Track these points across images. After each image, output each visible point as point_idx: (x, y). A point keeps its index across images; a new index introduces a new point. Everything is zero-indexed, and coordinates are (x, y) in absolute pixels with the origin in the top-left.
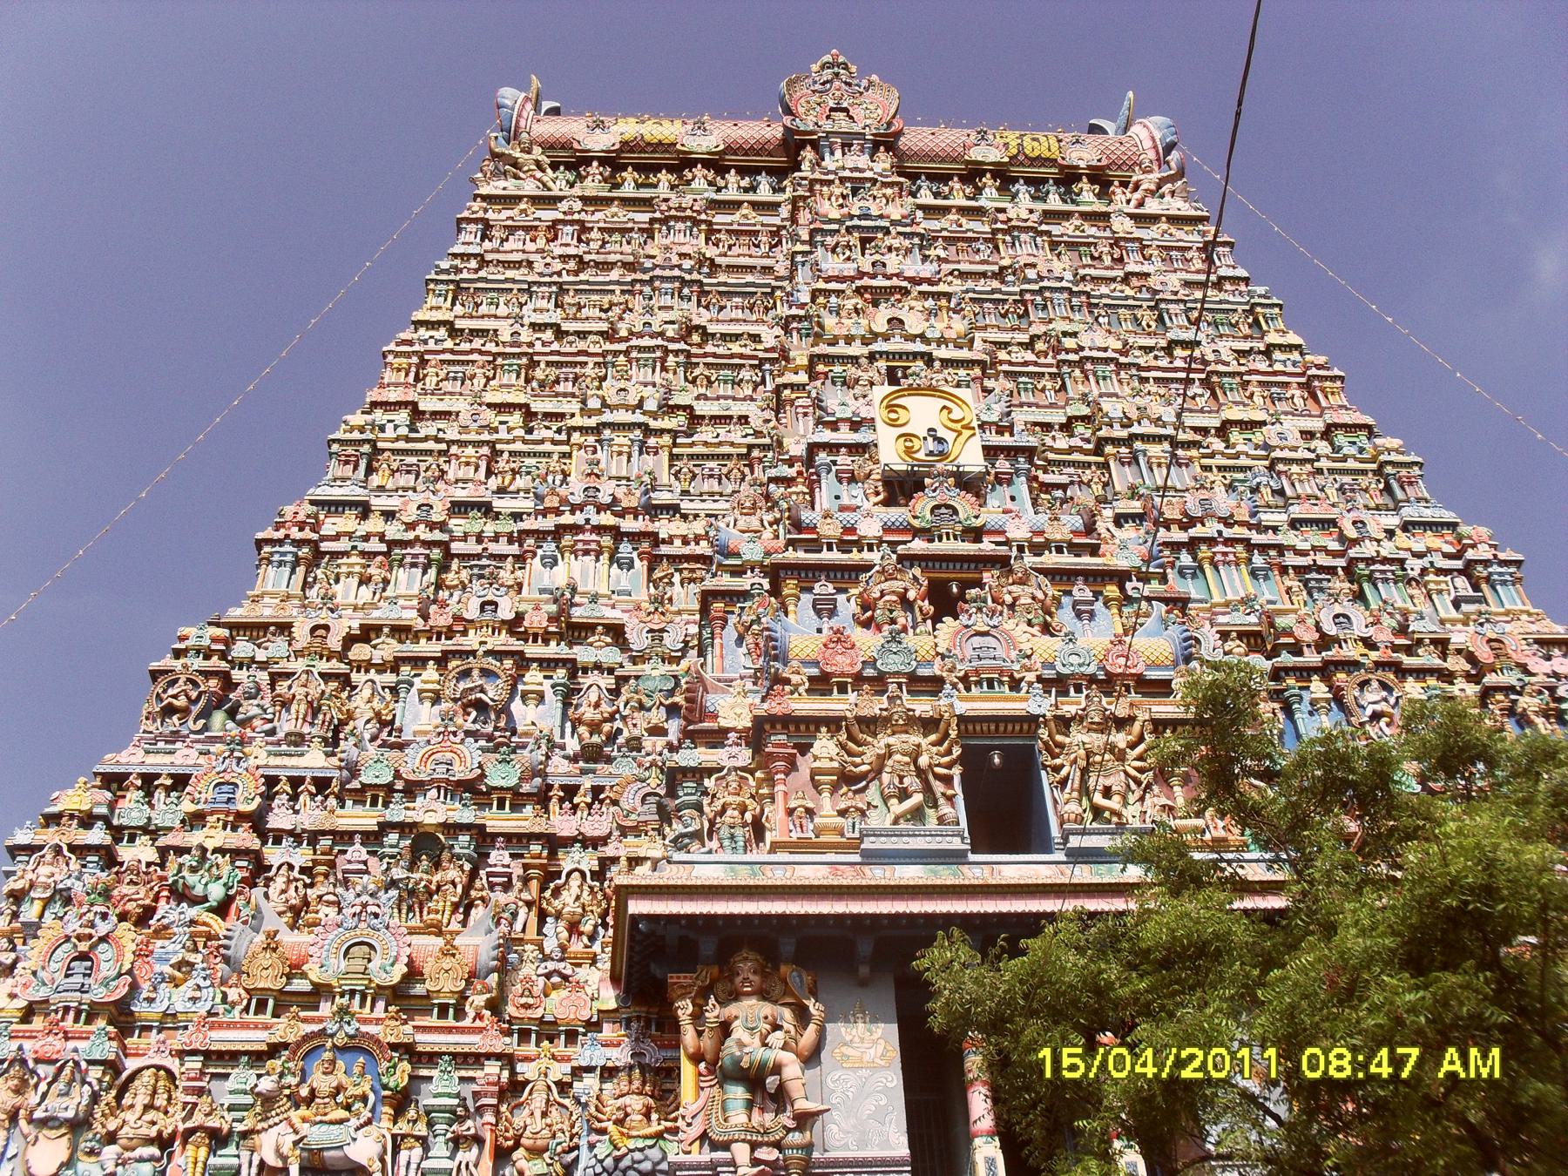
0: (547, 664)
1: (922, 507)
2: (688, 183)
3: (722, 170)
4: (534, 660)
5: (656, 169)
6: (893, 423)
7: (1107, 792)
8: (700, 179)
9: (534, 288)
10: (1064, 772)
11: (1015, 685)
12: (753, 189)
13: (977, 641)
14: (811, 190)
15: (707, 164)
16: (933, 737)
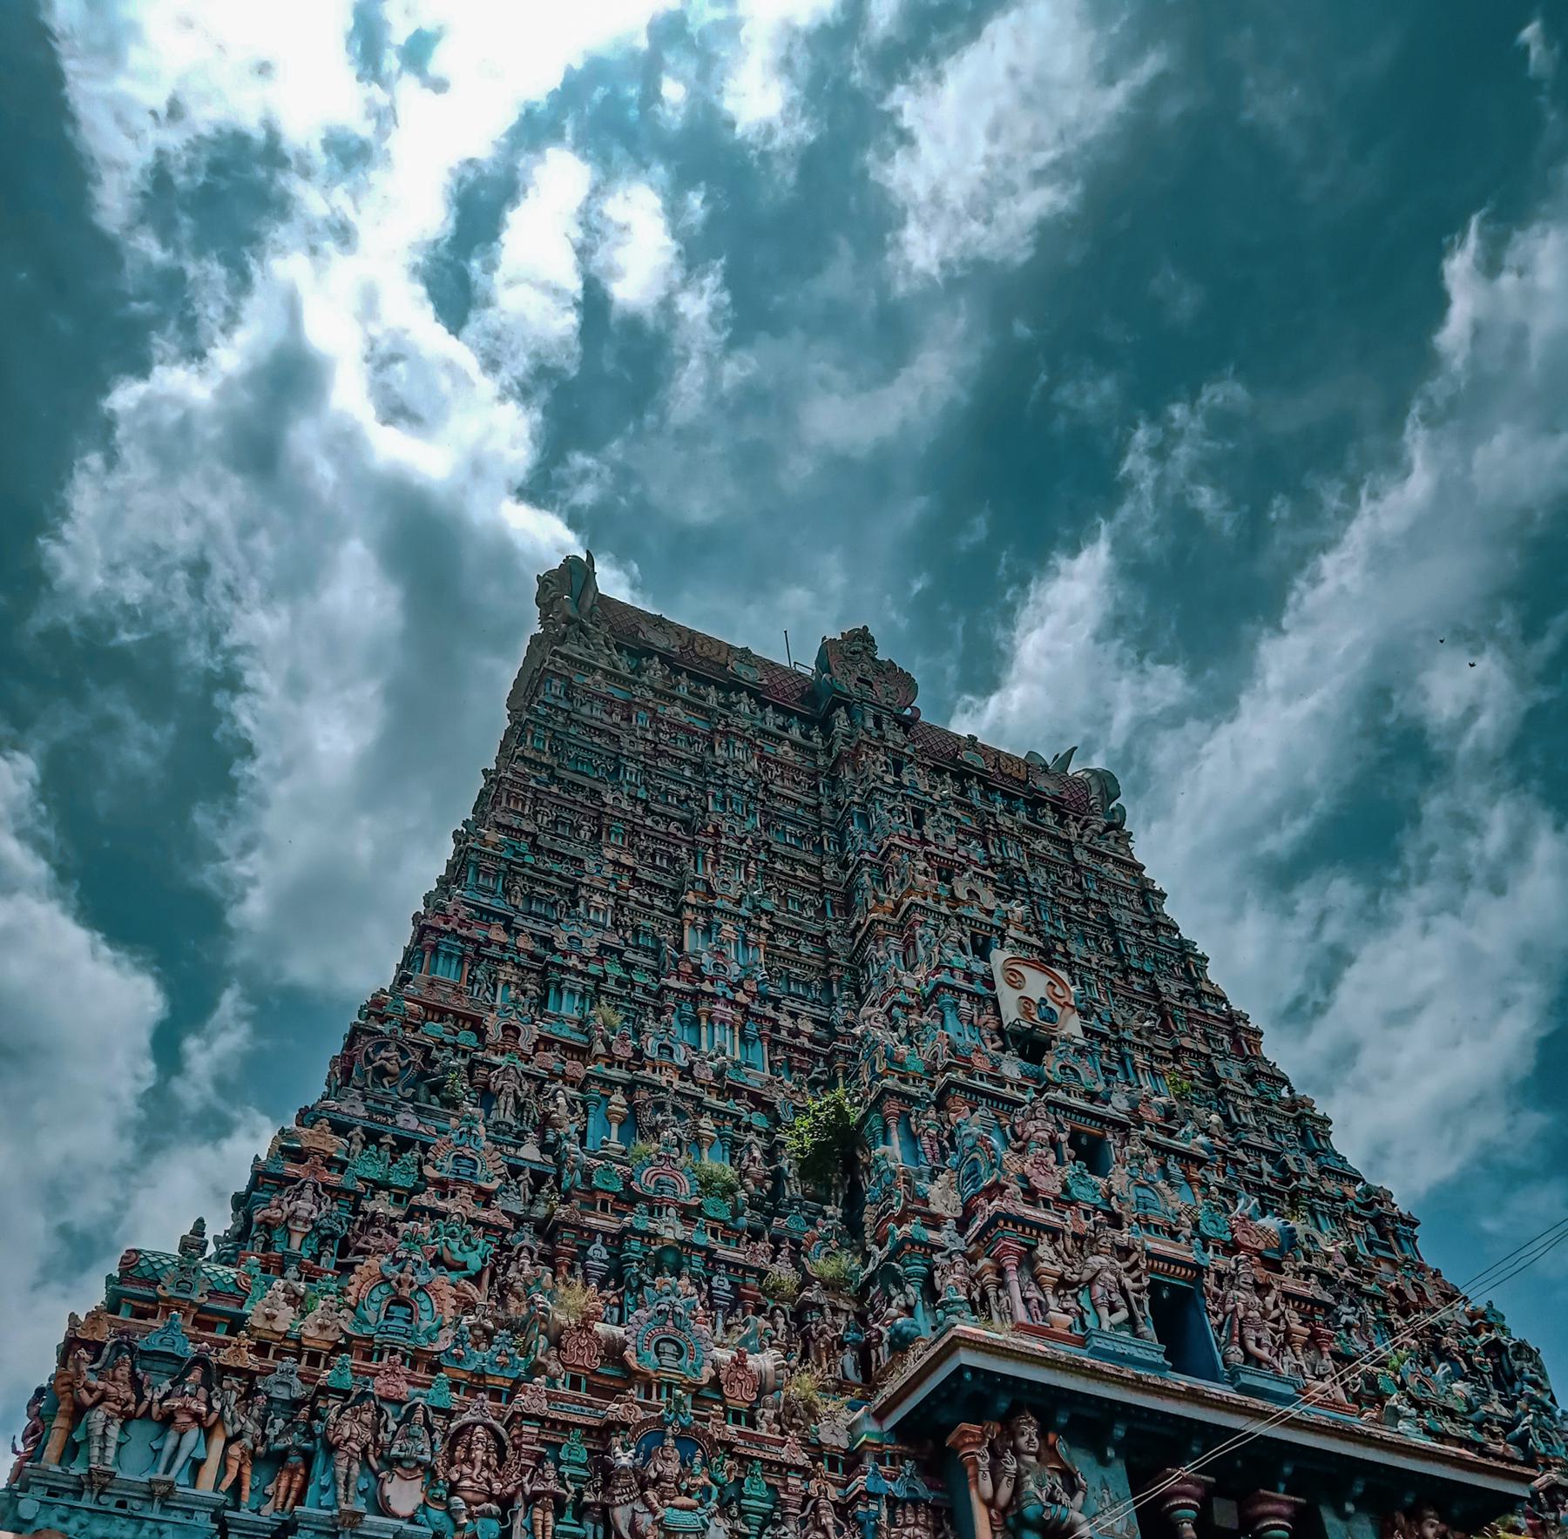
0: (717, 1113)
1: (1051, 1065)
2: (734, 704)
3: (763, 704)
4: (708, 1109)
5: (708, 682)
6: (1011, 983)
7: (1258, 1343)
8: (745, 705)
9: (623, 761)
10: (1221, 1317)
11: (1174, 1235)
12: (784, 728)
13: (1141, 1192)
14: (856, 749)
15: (752, 694)
16: (1127, 1264)
